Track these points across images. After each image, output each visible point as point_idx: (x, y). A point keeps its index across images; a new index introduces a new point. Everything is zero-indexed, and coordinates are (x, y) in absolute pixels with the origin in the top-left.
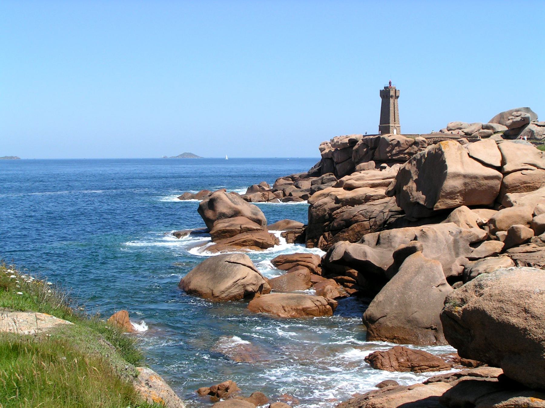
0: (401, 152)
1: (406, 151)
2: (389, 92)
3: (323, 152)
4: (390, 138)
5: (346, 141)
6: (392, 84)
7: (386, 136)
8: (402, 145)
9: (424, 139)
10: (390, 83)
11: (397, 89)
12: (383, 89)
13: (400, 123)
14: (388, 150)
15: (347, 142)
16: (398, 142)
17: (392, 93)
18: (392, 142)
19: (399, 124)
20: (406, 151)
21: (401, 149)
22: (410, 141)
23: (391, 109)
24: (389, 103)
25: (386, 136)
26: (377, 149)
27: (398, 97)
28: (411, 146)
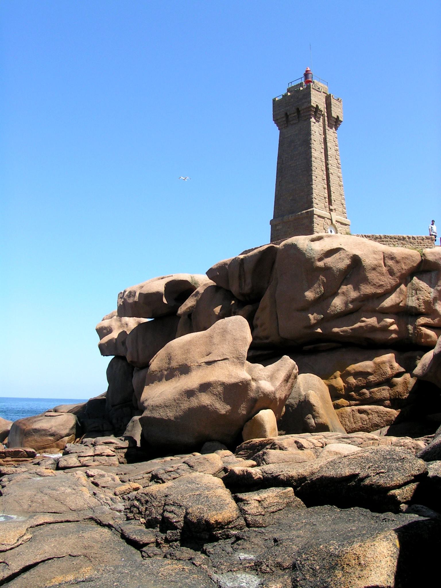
0: (367, 304)
1: (388, 302)
2: (307, 94)
3: (106, 339)
4: (319, 247)
7: (302, 241)
8: (371, 276)
14: (310, 295)
16: (356, 260)
18: (329, 261)
20: (388, 302)
21: (367, 289)
22: (406, 258)
24: (308, 133)
25: (302, 241)
26: (265, 301)
28: (406, 278)
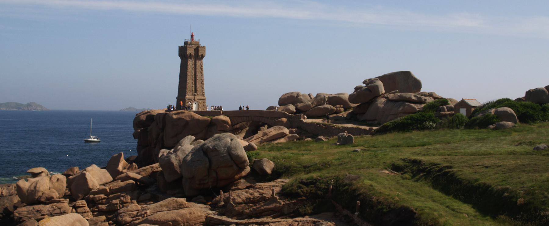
5: (143, 117)
6: (194, 38)
9: (227, 119)
10: (192, 36)
11: (202, 44)
12: (183, 45)
13: (206, 94)
15: (144, 119)
17: (190, 51)
19: (203, 95)
23: (188, 73)
27: (203, 57)
